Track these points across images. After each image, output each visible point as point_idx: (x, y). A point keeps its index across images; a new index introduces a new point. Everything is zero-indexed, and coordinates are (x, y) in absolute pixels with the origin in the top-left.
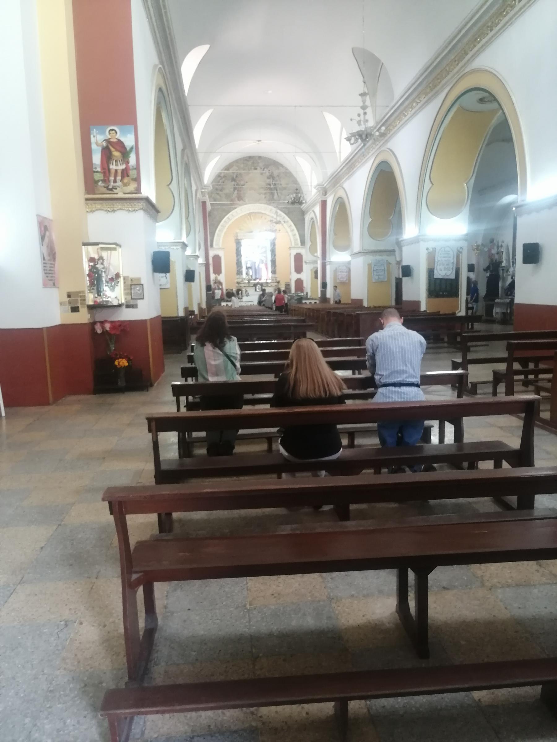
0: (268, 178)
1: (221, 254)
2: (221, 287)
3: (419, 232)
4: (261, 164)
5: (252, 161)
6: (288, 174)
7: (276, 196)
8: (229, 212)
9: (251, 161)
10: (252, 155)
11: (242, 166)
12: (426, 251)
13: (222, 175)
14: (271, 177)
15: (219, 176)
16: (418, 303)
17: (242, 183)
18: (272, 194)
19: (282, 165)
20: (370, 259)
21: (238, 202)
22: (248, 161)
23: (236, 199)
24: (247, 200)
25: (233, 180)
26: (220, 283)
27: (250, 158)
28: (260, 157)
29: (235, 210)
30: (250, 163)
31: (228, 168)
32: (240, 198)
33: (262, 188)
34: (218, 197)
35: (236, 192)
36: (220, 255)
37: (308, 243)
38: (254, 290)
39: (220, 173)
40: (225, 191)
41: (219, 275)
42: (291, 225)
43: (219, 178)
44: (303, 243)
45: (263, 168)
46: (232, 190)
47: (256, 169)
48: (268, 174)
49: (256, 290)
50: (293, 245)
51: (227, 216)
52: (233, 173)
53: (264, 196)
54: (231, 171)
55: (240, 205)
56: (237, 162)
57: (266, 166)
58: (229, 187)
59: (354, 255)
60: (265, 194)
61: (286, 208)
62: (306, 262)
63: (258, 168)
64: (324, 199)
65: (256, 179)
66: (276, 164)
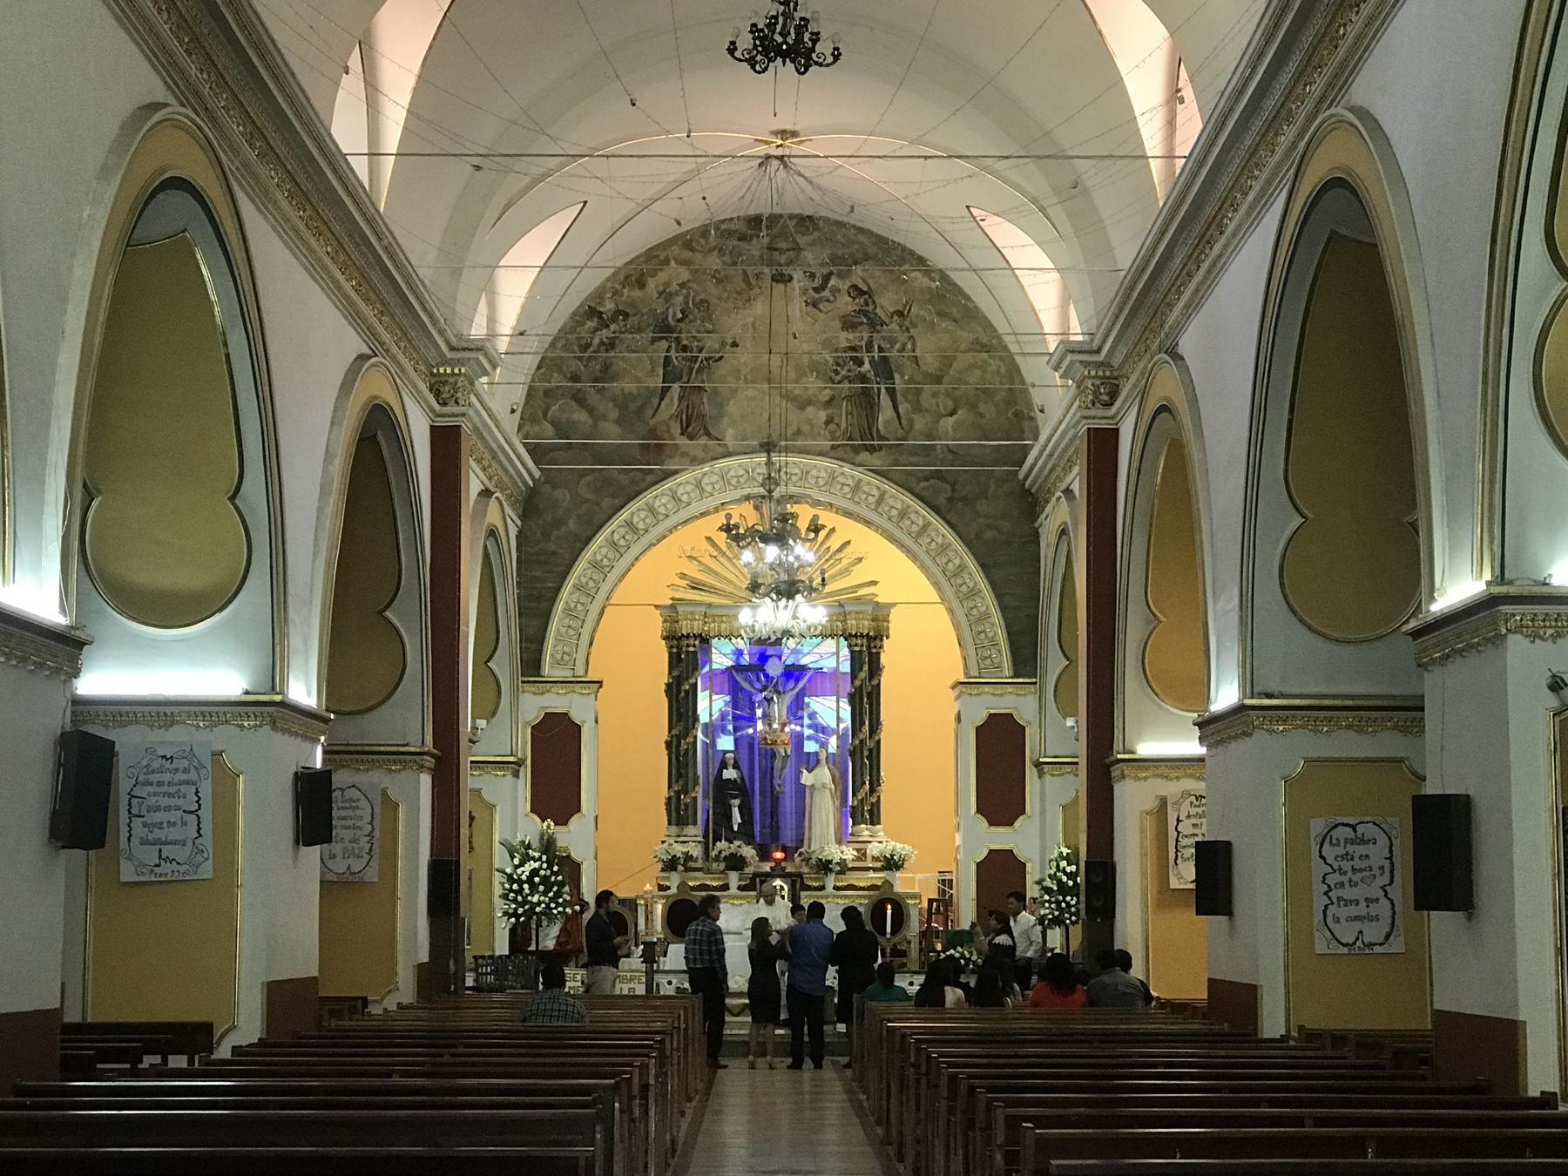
0: (848, 324)
1: (578, 707)
3: (1501, 577)
4: (813, 257)
6: (950, 300)
7: (886, 413)
9: (775, 242)
11: (714, 262)
12: (1552, 701)
13: (608, 306)
15: (590, 311)
16: (1504, 1037)
18: (867, 402)
19: (921, 261)
20: (1291, 749)
21: (683, 441)
23: (676, 429)
25: (664, 329)
26: (571, 869)
27: (755, 221)
28: (806, 222)
29: (668, 485)
30: (756, 248)
31: (635, 275)
32: (694, 423)
33: (814, 367)
34: (581, 416)
36: (576, 717)
37: (1053, 663)
39: (599, 295)
41: (562, 821)
42: (962, 568)
43: (591, 324)
44: (1025, 661)
46: (657, 382)
47: (782, 278)
48: (846, 304)
50: (974, 672)
51: (624, 515)
52: (666, 295)
53: (822, 415)
54: (652, 284)
55: (695, 461)
56: (687, 242)
57: (842, 263)
59: (1210, 727)
60: (829, 402)
61: (938, 475)
62: (1038, 765)
64: (1103, 424)
65: (782, 334)
66: (894, 256)
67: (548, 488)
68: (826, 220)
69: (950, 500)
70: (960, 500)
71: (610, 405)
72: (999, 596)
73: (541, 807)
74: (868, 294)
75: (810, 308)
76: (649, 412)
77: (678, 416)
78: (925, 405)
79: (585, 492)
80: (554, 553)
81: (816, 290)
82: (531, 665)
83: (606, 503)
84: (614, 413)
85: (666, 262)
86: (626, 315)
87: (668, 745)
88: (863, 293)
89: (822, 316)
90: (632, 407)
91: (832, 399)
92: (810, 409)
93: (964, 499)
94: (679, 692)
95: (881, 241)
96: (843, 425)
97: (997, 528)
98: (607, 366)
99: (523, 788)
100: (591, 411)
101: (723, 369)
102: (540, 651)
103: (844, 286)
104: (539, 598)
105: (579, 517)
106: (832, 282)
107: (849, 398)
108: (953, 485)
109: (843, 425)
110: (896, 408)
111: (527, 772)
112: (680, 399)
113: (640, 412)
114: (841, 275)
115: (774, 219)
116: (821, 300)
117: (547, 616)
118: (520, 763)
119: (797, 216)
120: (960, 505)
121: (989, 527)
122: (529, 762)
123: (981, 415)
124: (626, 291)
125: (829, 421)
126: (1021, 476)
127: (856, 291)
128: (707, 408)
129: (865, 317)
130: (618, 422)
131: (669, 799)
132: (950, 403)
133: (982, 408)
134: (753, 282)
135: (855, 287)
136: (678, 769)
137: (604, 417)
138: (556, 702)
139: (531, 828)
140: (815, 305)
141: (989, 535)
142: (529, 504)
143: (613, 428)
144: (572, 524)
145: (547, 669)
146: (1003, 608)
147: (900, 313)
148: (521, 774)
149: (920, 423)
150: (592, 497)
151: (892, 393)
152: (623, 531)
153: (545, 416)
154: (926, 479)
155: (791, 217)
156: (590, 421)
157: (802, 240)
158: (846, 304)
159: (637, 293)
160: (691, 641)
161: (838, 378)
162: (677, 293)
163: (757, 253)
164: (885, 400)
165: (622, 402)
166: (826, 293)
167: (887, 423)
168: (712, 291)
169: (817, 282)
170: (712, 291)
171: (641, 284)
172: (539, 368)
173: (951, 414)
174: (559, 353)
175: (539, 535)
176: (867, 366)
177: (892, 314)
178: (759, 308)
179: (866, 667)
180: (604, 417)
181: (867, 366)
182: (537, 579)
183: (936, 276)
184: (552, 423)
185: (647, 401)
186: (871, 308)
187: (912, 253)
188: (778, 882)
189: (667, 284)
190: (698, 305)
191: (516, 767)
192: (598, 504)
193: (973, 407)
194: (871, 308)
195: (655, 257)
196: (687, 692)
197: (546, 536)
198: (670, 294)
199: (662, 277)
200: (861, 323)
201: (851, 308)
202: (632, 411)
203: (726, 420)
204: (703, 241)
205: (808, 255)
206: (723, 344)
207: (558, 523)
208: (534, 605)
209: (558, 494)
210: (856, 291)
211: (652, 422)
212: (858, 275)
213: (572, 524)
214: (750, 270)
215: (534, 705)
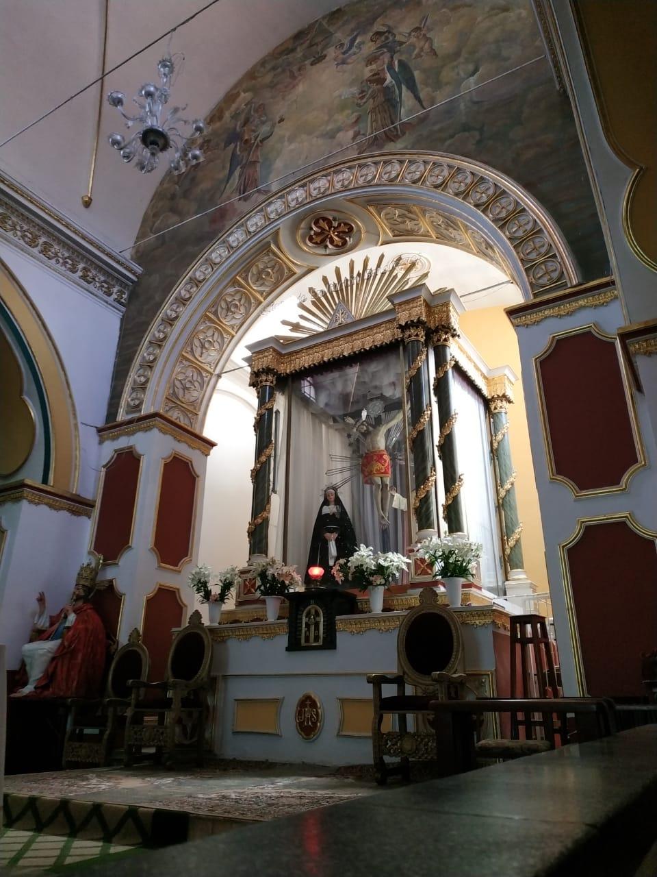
22: (293, 50)
48: (369, 48)
54: (227, 115)
85: (238, 94)
101: (270, 143)
110: (417, 98)
132: (471, 67)
151: (412, 87)
154: (452, 136)
158: (369, 48)
166: (354, 49)
171: (220, 118)
174: (165, 186)
176: (389, 78)
178: (301, 88)
194: (391, 39)
201: (373, 48)
204: (262, 69)
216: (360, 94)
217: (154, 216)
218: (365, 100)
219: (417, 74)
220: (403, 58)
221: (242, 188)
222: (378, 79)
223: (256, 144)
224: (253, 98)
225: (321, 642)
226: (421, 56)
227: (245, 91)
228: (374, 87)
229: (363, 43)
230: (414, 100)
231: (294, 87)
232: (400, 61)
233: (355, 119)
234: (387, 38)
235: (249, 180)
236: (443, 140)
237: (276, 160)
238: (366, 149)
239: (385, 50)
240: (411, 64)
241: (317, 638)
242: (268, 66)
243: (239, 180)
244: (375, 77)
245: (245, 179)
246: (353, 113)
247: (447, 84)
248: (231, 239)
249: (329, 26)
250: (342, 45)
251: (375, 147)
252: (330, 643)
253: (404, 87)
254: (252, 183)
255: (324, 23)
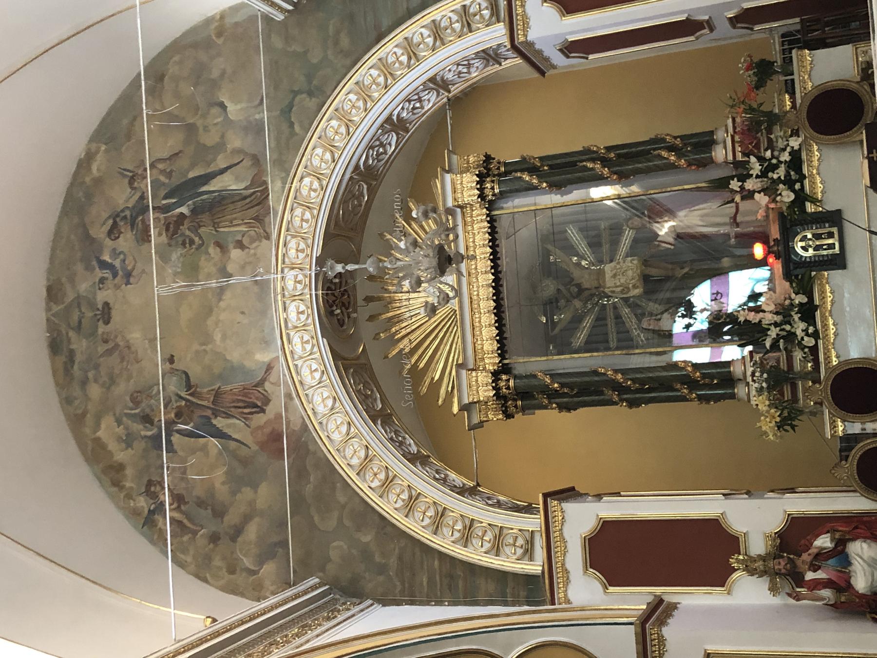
2: (824, 542)
5: (71, 334)
8: (329, 473)
10: (40, 336)
11: (95, 391)
13: (143, 503)
14: (133, 219)
15: (148, 523)
17: (174, 386)
19: (84, 164)
21: (271, 410)
22: (71, 354)
23: (259, 419)
24: (263, 357)
27: (55, 346)
28: (53, 293)
30: (80, 345)
31: (111, 474)
32: (252, 400)
34: (252, 532)
35: (219, 422)
38: (836, 276)
39: (133, 514)
40: (222, 490)
45: (99, 273)
47: (106, 313)
48: (126, 241)
49: (838, 262)
52: (128, 441)
53: (235, 254)
54: (121, 455)
58: (201, 465)
63: (102, 296)
67: (329, 567)
68: (50, 272)
69: (310, 94)
70: (310, 82)
71: (239, 496)
72: (410, 14)
73: (717, 576)
74: (115, 216)
75: (132, 280)
76: (244, 452)
77: (246, 418)
78: (217, 140)
79: (331, 523)
80: (400, 558)
81: (115, 275)
82: (535, 590)
83: (341, 498)
84: (247, 493)
85: (97, 440)
86: (150, 483)
87: (633, 404)
88: (115, 225)
89: (139, 265)
90: (239, 471)
91: (218, 244)
92: (230, 268)
93: (310, 78)
94: (564, 395)
95: (65, 212)
96: (243, 228)
97: (338, 32)
98: (201, 503)
99: (692, 599)
100: (247, 519)
101: (196, 372)
102: (516, 575)
103: (108, 242)
104: (451, 577)
105: (358, 529)
106: (107, 258)
107: (216, 226)
108: (296, 93)
109: (243, 228)
111: (671, 593)
112: (229, 416)
113: (245, 462)
114: (100, 249)
115: (51, 327)
116: (124, 268)
117: (472, 568)
118: (659, 602)
119: (47, 304)
120: (315, 82)
121: (336, 43)
122: (658, 590)
123: (223, 73)
124: (128, 484)
125: (240, 245)
126: (280, 17)
127: (113, 232)
128: (233, 386)
129: (133, 219)
130: (255, 487)
131: (700, 398)
132: (215, 110)
133: (215, 74)
134: (110, 345)
135: (110, 233)
136: (590, 394)
137: (251, 503)
138: (574, 557)
139: (749, 592)
140: (128, 275)
141: (345, 42)
142: (350, 591)
143: (264, 490)
144: (367, 538)
145: (535, 567)
146: (423, 6)
147: (132, 180)
148: (674, 599)
149: (235, 141)
150: (336, 514)
151: (207, 178)
152: (369, 476)
153: (254, 573)
154: (292, 125)
155: (48, 309)
156: (257, 520)
157: (71, 296)
158: (126, 241)
159: (129, 471)
160: (502, 384)
161: (197, 239)
162: (126, 428)
163: (84, 343)
164: (214, 185)
165: (236, 482)
166: (117, 263)
167: (237, 179)
168: (122, 388)
169: (107, 274)
170: (122, 388)
171: (120, 468)
172: (205, 580)
173: (223, 106)
174: (189, 559)
175: (381, 578)
176: (184, 210)
177: (133, 188)
179: (519, 174)
180: (251, 503)
181: (184, 210)
182: (431, 581)
183: (94, 146)
184: (261, 564)
185: (234, 455)
186: (128, 213)
187: (76, 175)
188: (798, 246)
189: (119, 439)
190: (136, 403)
191: (658, 613)
192: (343, 507)
193: (215, 85)
194: (128, 213)
195: (95, 454)
196: (562, 385)
197: (382, 569)
198: (128, 435)
199: (112, 446)
200: (143, 221)
202: (244, 473)
203: (248, 364)
204: (77, 402)
205: (83, 287)
206: (173, 371)
207: (366, 554)
208: (461, 584)
209: (334, 554)
210: (113, 232)
211: (255, 447)
212: (99, 232)
213: (367, 538)
214: (101, 349)
215: (583, 589)
216: (185, 247)
217: (232, 571)
218: (197, 239)
219: (191, 175)
220: (162, 193)
221: (246, 411)
222: (172, 228)
223: (188, 397)
224: (115, 415)
225: (835, 230)
226: (171, 171)
227: (97, 426)
228: (185, 229)
229: (115, 253)
230: (224, 175)
231: (129, 347)
232: (165, 198)
233: (218, 249)
234: (125, 217)
235: (239, 401)
236: (293, 134)
237: (226, 360)
238: (265, 231)
239: (141, 218)
240: (176, 181)
241: (831, 235)
242: (77, 391)
243: (233, 417)
244: (171, 230)
245: (236, 407)
246: (207, 253)
247: (223, 137)
248: (321, 409)
249: (63, 303)
250: (102, 280)
251: (266, 220)
252: (835, 218)
253: (205, 188)
254: (245, 395)
255: (56, 308)
